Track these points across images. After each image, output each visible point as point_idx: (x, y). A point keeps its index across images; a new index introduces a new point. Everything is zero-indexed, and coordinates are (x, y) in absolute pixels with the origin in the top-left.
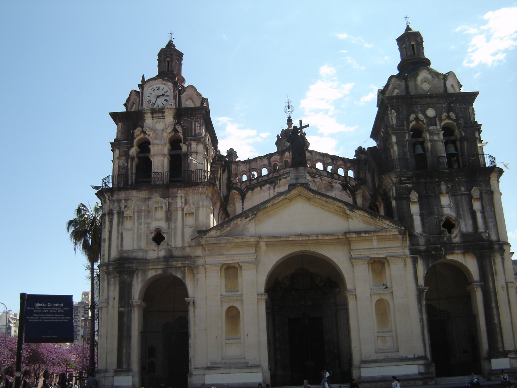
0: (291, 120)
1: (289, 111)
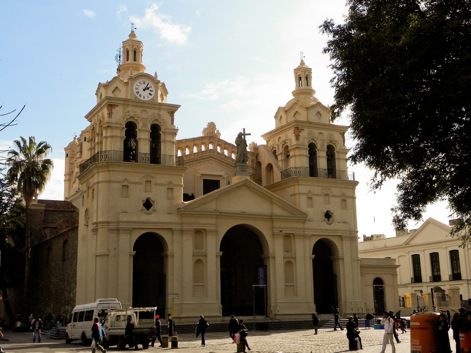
1: (120, 60)
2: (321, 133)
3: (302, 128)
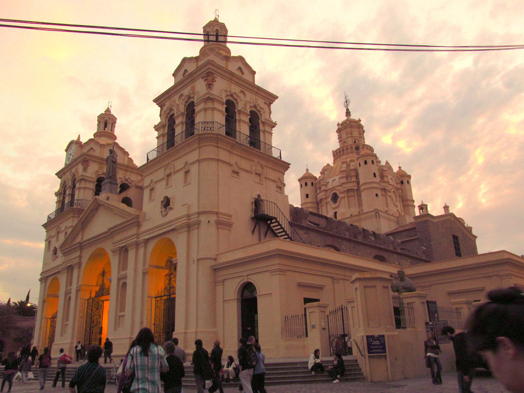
0: (350, 112)
1: (347, 105)
2: (182, 95)
3: (163, 104)
